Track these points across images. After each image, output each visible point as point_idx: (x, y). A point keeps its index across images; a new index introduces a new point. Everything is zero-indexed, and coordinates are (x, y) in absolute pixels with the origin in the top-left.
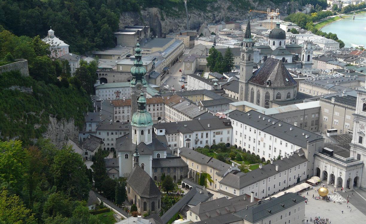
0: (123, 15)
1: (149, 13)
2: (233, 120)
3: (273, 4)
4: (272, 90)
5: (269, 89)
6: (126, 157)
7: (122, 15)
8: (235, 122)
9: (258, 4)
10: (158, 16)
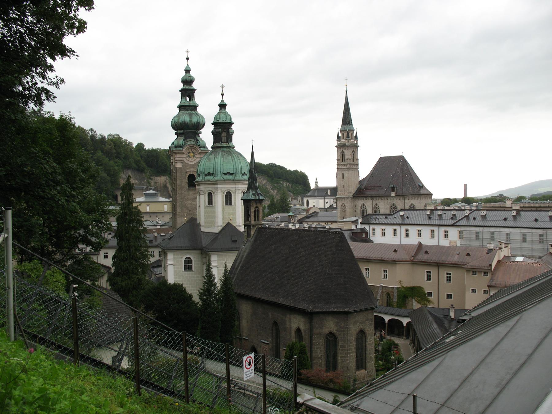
0: (125, 173)
1: (156, 183)
2: (372, 227)
3: (292, 194)
4: (401, 199)
5: (395, 200)
6: (186, 268)
7: (123, 173)
8: (378, 229)
9: (277, 193)
10: (168, 187)
